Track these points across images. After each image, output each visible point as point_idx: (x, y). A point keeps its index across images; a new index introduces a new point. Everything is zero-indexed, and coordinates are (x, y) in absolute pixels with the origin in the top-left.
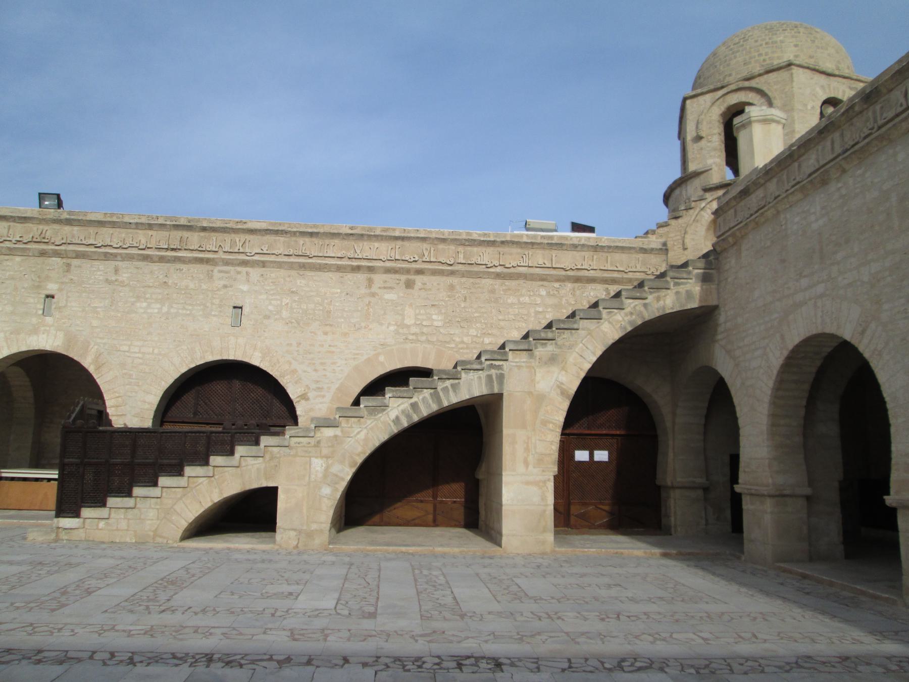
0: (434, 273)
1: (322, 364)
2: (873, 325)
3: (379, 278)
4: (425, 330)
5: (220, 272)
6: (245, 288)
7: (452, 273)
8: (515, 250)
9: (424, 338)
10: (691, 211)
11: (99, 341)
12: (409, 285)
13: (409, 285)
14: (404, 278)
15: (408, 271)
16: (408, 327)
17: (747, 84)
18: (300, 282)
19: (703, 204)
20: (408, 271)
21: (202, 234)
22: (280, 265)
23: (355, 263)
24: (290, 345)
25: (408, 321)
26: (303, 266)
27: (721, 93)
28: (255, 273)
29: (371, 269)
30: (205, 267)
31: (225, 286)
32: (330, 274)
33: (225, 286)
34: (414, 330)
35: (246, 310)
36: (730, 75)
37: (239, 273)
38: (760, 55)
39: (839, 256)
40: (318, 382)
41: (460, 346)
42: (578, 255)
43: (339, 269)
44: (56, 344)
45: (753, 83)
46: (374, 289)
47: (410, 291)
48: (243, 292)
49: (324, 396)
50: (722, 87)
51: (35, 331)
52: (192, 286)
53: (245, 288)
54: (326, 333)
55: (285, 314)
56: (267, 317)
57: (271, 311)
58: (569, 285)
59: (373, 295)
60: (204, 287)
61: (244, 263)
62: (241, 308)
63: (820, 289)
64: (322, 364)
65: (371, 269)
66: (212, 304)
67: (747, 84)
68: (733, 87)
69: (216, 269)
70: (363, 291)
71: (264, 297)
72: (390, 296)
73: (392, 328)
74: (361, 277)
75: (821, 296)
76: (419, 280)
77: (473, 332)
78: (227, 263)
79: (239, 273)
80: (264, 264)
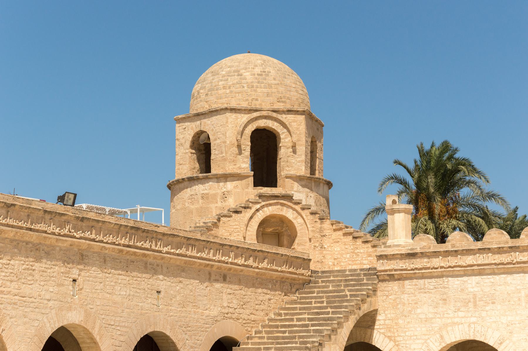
2: (508, 342)
4: (231, 310)
10: (248, 210)
11: (100, 316)
16: (225, 308)
19: (258, 206)
25: (225, 304)
27: (255, 114)
29: (212, 266)
36: (257, 100)
38: (278, 92)
39: (487, 308)
41: (244, 322)
44: (80, 319)
45: (279, 117)
50: (256, 111)
51: (70, 309)
57: (172, 295)
63: (473, 319)
67: (275, 115)
68: (264, 113)
75: (474, 323)
77: (248, 312)
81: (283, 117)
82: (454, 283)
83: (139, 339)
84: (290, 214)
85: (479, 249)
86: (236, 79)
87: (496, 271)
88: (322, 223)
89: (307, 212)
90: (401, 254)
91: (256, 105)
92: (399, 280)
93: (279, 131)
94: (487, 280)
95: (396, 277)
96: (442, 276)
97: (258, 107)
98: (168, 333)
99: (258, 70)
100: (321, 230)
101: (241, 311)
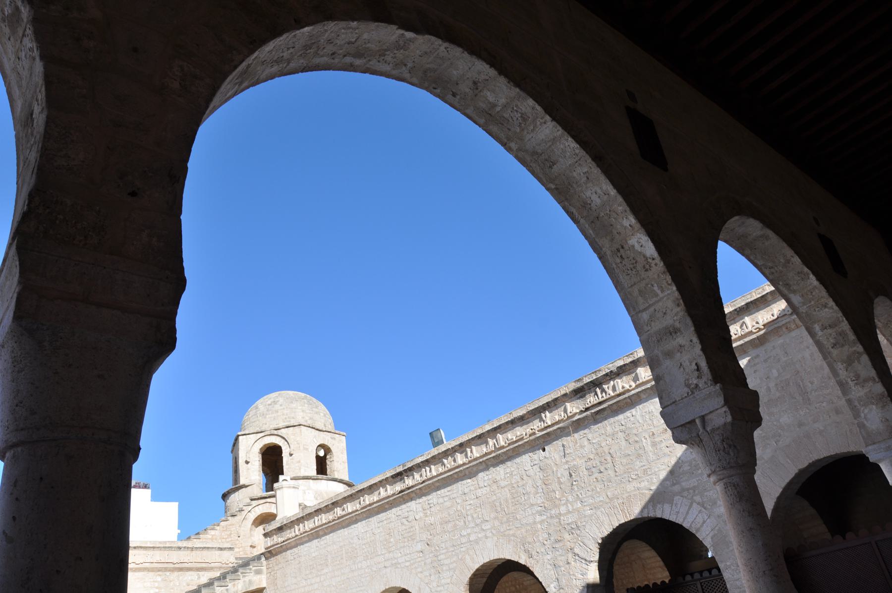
17: (276, 432)
19: (250, 508)
45: (279, 432)
58: (176, 573)
67: (276, 432)
68: (268, 433)
81: (283, 432)
93: (280, 444)
96: (296, 546)
97: (263, 429)
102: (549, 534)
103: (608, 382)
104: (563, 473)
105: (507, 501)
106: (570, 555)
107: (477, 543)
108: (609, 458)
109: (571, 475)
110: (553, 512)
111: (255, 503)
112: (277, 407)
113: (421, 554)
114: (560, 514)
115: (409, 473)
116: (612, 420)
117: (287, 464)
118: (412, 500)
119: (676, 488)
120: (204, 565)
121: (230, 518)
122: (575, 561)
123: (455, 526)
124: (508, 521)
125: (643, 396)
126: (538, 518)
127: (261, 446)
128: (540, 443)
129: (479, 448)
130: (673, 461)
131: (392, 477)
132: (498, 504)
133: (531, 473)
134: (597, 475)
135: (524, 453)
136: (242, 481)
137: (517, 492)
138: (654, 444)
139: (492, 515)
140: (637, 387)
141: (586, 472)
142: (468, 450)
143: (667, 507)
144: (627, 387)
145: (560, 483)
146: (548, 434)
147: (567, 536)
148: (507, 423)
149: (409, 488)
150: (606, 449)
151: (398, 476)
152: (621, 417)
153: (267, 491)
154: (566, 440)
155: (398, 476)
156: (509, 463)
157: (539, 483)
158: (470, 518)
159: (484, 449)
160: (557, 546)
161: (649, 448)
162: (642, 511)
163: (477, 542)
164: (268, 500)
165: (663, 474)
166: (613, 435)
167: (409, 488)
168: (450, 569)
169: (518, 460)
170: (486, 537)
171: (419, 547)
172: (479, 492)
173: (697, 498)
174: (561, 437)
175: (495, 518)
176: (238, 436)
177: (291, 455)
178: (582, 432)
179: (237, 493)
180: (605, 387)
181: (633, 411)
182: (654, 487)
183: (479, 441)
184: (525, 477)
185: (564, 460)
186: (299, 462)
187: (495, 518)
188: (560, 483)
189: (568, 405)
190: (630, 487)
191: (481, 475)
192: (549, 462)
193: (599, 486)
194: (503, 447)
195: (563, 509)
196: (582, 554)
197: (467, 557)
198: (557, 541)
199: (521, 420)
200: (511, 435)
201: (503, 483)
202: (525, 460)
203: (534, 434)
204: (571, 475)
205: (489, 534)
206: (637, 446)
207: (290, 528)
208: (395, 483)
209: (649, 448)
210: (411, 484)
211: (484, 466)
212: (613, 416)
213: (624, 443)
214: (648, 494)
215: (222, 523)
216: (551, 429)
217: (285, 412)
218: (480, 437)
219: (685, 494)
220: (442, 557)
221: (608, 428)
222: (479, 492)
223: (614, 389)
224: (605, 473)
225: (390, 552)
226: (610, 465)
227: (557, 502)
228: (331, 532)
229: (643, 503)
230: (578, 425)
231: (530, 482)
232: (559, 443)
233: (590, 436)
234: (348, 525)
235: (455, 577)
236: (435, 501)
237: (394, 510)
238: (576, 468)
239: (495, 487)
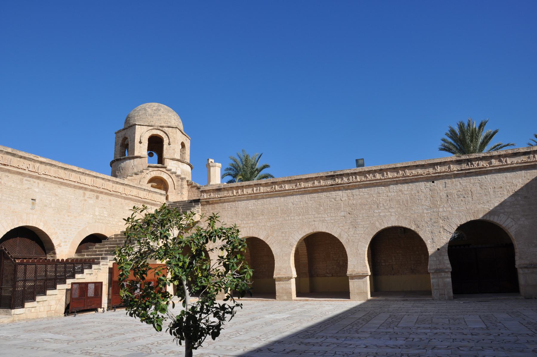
0: (106, 194)
1: (67, 230)
3: (88, 193)
4: (102, 218)
5: (26, 180)
6: (37, 190)
7: (111, 195)
8: (128, 188)
9: (101, 221)
12: (97, 197)
13: (97, 197)
14: (96, 194)
15: (98, 192)
16: (96, 216)
17: (161, 128)
18: (60, 191)
19: (148, 171)
20: (98, 192)
21: (19, 159)
22: (52, 181)
23: (81, 185)
24: (55, 220)
25: (97, 214)
26: (62, 183)
28: (42, 183)
29: (86, 189)
30: (20, 177)
31: (28, 188)
32: (69, 189)
33: (28, 188)
34: (98, 217)
35: (37, 201)
37: (34, 182)
39: (259, 218)
40: (65, 238)
42: (145, 193)
43: (75, 187)
46: (86, 198)
47: (97, 200)
48: (36, 192)
49: (67, 245)
52: (13, 186)
53: (37, 190)
54: (68, 216)
55: (53, 205)
56: (46, 206)
59: (85, 200)
60: (19, 187)
61: (38, 178)
62: (35, 200)
64: (67, 230)
65: (86, 189)
66: (23, 196)
67: (161, 128)
68: (156, 127)
69: (25, 178)
70: (82, 198)
71: (44, 196)
72: (91, 202)
73: (91, 216)
74: (81, 191)
76: (101, 196)
77: (116, 220)
78: (31, 176)
79: (34, 182)
80: (46, 180)
81: (166, 129)
82: (242, 204)
83: (9, 230)
84: (165, 176)
85: (255, 185)
86: (144, 111)
87: (264, 196)
88: (182, 181)
89: (174, 175)
90: (213, 190)
91: (153, 124)
92: (212, 204)
93: (163, 136)
94: (260, 202)
95: (210, 202)
96: (234, 201)
97: (153, 125)
98: (41, 228)
99: (154, 108)
100: (182, 185)
101: (111, 219)
102: (431, 219)
103: (476, 161)
104: (443, 194)
105: (407, 201)
106: (441, 230)
107: (385, 217)
108: (470, 193)
109: (447, 196)
110: (435, 210)
111: (151, 169)
112: (160, 113)
113: (343, 218)
114: (439, 211)
115: (339, 177)
116: (474, 177)
117: (166, 149)
118: (339, 190)
119: (502, 211)
120: (155, 202)
121: (134, 175)
122: (444, 232)
123: (371, 207)
124: (407, 209)
125: (493, 171)
126: (425, 211)
127: (150, 135)
128: (433, 179)
129: (392, 174)
130: (503, 200)
131: (326, 176)
132: (401, 201)
133: (425, 191)
134: (462, 198)
135: (421, 181)
136: (136, 154)
137: (414, 198)
138: (494, 192)
139: (397, 206)
140: (490, 167)
141: (456, 196)
142: (385, 173)
143: (496, 218)
144: (485, 166)
145: (441, 198)
146: (439, 176)
147: (441, 221)
148: (414, 166)
149: (338, 184)
150: (469, 189)
151: (332, 177)
152: (479, 177)
153: (158, 163)
154: (446, 181)
155: (332, 177)
156: (411, 184)
157: (429, 196)
158: (381, 205)
159: (395, 175)
160: (435, 224)
161: (492, 193)
162: (483, 217)
163: (385, 216)
164: (160, 169)
165: (496, 204)
166: (474, 184)
167: (338, 184)
168: (364, 227)
169: (417, 184)
170: (391, 215)
171: (343, 214)
172: (390, 194)
173: (512, 216)
174: (445, 179)
175: (398, 207)
176: (136, 125)
177: (169, 144)
178: (457, 179)
179: (132, 161)
180: (474, 163)
181: (486, 176)
182: (491, 209)
183: (393, 170)
184: (420, 192)
185: (445, 189)
186: (174, 150)
187: (398, 207)
188: (441, 198)
189: (451, 166)
190: (479, 207)
191: (391, 186)
192: (436, 188)
193: (462, 203)
194: (408, 176)
195: (441, 210)
196: (448, 230)
197: (377, 222)
198: (435, 222)
199: (422, 166)
200: (414, 172)
201: (406, 193)
202: (422, 185)
203: (429, 174)
204: (447, 196)
205: (393, 214)
206: (486, 191)
207: (228, 190)
208: (327, 180)
209: (492, 193)
210: (340, 182)
211: (395, 182)
212: (475, 176)
213: (479, 188)
214: (488, 211)
215: (128, 177)
216: (442, 174)
217: (166, 117)
218: (394, 168)
219: (506, 213)
220: (359, 221)
221: (472, 180)
222: (390, 194)
223: (478, 165)
224: (467, 199)
225: (319, 214)
226: (470, 196)
227: (438, 206)
228: (268, 198)
229: (484, 214)
230: (456, 176)
231: (423, 194)
232: (443, 181)
233: (461, 182)
234: (284, 196)
235: (367, 231)
236: (357, 193)
237: (325, 193)
238: (451, 194)
239: (400, 193)
